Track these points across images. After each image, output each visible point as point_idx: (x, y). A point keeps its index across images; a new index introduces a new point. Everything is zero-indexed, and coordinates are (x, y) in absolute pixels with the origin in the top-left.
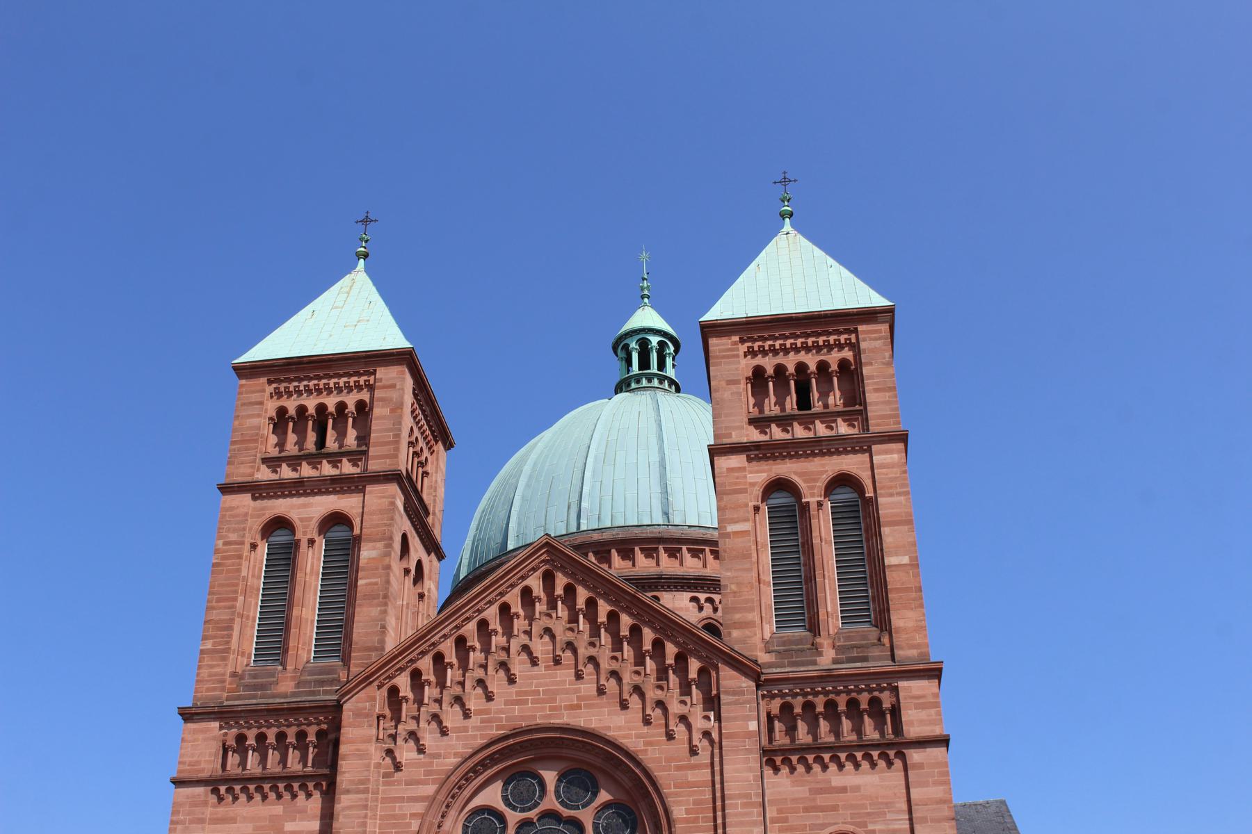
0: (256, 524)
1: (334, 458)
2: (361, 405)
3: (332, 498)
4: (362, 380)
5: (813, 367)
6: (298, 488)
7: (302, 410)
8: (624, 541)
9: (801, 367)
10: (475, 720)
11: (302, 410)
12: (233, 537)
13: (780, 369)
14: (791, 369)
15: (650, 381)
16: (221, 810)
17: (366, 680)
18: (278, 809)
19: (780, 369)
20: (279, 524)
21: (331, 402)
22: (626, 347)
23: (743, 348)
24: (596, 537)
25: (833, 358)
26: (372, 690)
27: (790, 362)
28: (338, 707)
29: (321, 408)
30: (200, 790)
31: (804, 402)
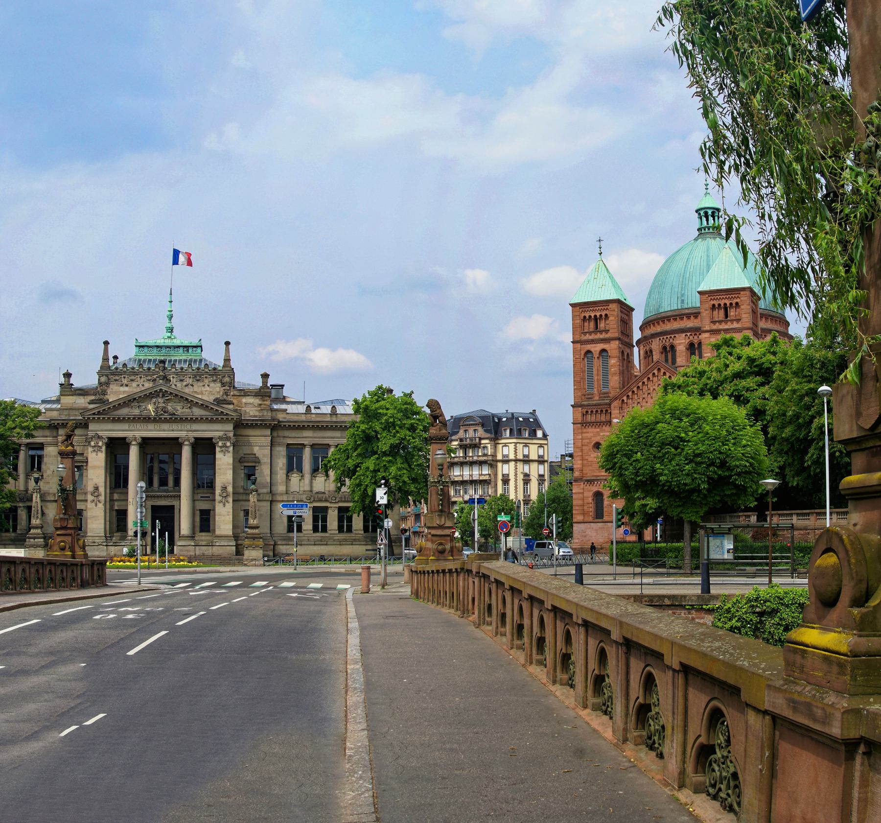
0: (583, 352)
1: (601, 332)
2: (606, 315)
3: (602, 344)
4: (606, 307)
5: (728, 305)
6: (592, 341)
7: (590, 317)
8: (695, 313)
9: (725, 304)
10: (643, 408)
11: (590, 317)
12: (577, 357)
13: (719, 305)
14: (722, 305)
15: (709, 229)
16: (585, 430)
17: (616, 399)
18: (598, 430)
19: (719, 305)
20: (589, 352)
21: (598, 314)
22: (700, 214)
23: (709, 298)
24: (687, 311)
25: (734, 301)
26: (618, 401)
27: (722, 303)
28: (610, 404)
29: (595, 316)
30: (579, 425)
31: (726, 316)
